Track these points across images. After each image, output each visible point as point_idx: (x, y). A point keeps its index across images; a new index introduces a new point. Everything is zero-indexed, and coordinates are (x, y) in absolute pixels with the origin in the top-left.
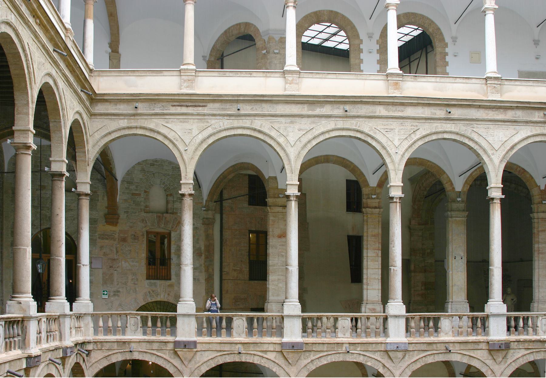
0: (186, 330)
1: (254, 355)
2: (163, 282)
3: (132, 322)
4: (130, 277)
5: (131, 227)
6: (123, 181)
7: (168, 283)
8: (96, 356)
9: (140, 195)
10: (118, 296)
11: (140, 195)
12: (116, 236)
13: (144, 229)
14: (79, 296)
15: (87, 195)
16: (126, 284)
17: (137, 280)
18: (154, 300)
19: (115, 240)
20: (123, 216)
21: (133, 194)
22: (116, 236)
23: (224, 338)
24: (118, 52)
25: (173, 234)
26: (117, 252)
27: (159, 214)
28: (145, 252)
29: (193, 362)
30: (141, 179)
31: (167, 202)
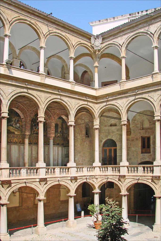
0: (124, 171)
1: (144, 180)
2: (147, 154)
3: (109, 169)
4: (135, 153)
5: (135, 136)
6: (132, 120)
7: (150, 154)
8: (99, 180)
9: (138, 124)
10: (131, 160)
11: (138, 124)
12: (130, 139)
13: (140, 136)
14: (95, 161)
15: (97, 129)
16: (133, 155)
17: (138, 154)
18: (144, 161)
19: (130, 141)
20: (132, 132)
21: (136, 124)
22: (130, 139)
23: (135, 174)
24: (129, 76)
25: (151, 137)
26: (130, 145)
27: (146, 130)
28: (141, 144)
29: (125, 182)
30: (139, 118)
31: (150, 125)
